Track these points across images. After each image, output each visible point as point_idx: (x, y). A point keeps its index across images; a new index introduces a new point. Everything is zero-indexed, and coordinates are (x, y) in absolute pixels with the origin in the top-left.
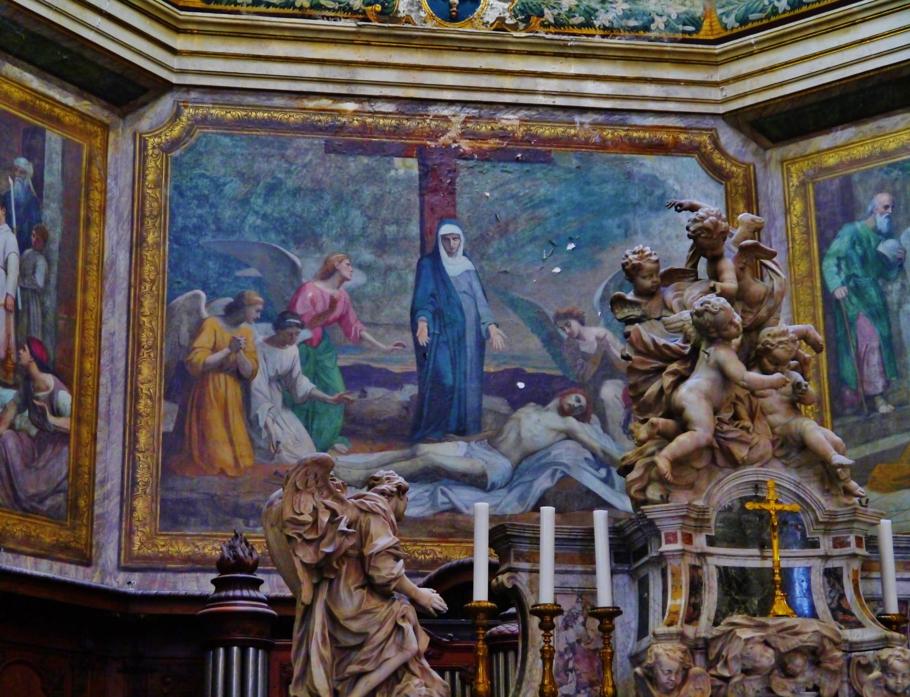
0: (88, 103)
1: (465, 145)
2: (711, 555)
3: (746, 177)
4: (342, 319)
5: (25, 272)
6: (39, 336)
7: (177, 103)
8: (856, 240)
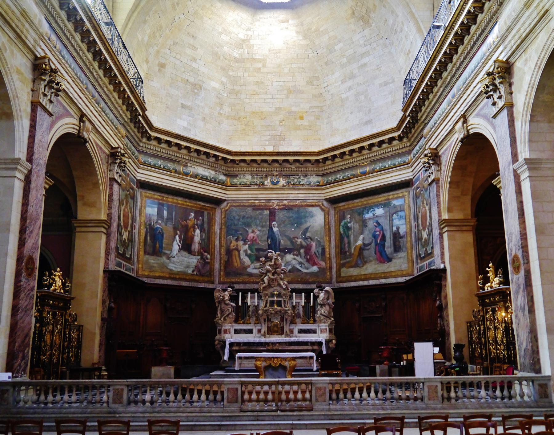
1: (277, 207)
4: (255, 240)
5: (201, 236)
8: (345, 223)
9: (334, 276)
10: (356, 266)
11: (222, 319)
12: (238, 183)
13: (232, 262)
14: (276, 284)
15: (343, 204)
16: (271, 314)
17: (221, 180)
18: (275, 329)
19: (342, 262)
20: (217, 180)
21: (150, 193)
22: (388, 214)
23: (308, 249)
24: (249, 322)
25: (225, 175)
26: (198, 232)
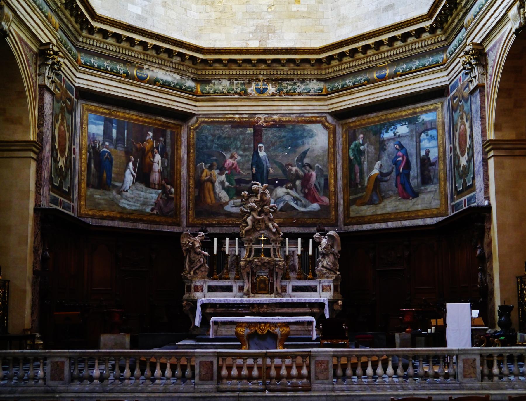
1: (265, 124)
3: (333, 128)
4: (235, 168)
5: (163, 163)
7: (197, 118)
8: (356, 145)
9: (341, 217)
10: (371, 202)
11: (192, 273)
12: (211, 91)
13: (204, 197)
14: (263, 226)
15: (354, 119)
16: (257, 266)
17: (189, 87)
18: (262, 285)
19: (351, 197)
20: (184, 88)
21: (93, 106)
22: (414, 133)
23: (306, 179)
24: (226, 276)
25: (194, 80)
26: (158, 157)
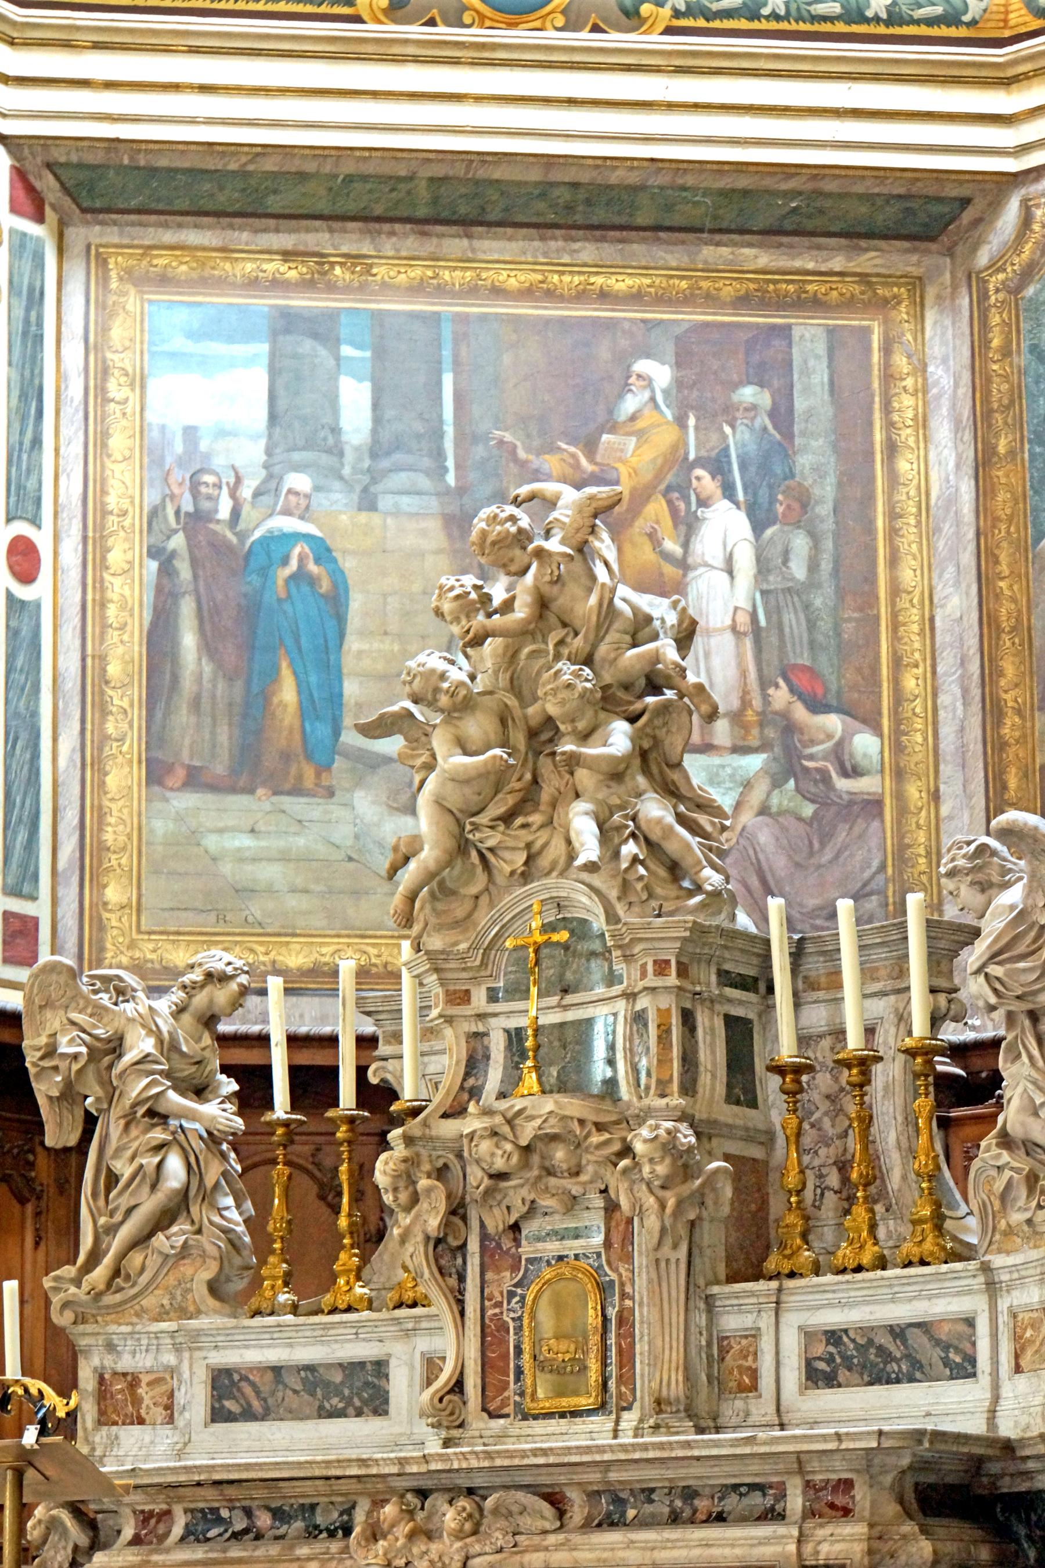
0: (873, 254)
2: (495, 1015)
6: (805, 660)
26: (725, 527)
